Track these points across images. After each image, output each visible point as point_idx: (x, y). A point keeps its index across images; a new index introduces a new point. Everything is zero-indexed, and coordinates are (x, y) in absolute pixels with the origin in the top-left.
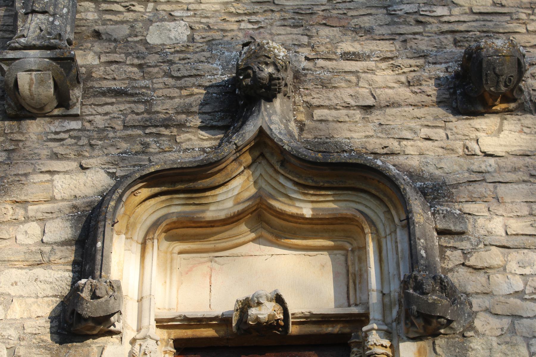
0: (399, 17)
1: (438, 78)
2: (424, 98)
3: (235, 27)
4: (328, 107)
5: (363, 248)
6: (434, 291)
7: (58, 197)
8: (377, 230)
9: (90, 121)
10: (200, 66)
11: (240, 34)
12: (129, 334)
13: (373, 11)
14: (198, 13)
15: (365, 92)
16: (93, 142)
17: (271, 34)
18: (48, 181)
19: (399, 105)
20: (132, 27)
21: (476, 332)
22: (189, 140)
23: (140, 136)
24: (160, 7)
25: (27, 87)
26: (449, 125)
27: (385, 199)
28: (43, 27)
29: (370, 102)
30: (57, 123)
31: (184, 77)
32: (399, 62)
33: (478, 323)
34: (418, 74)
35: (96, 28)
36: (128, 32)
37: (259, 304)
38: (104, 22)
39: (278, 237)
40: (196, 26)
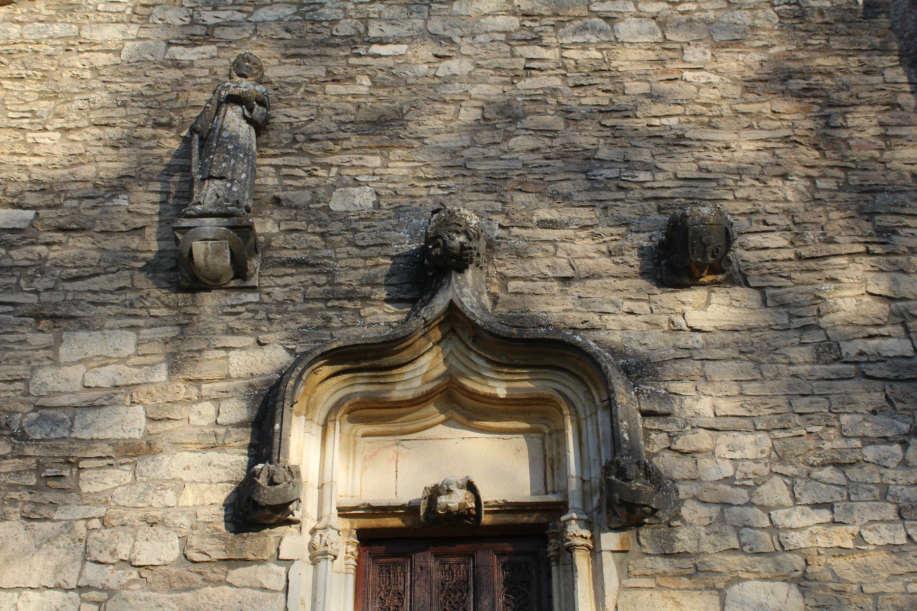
0: (599, 182)
1: (641, 248)
2: (627, 269)
4: (524, 279)
5: (562, 431)
6: (638, 477)
7: (234, 375)
8: (577, 412)
9: (268, 294)
10: (387, 234)
11: (430, 201)
12: (309, 524)
13: (572, 176)
14: (385, 178)
15: (563, 262)
16: (271, 316)
18: (223, 358)
19: (600, 277)
20: (314, 192)
21: (683, 521)
22: (375, 313)
23: (321, 309)
24: (344, 172)
25: (202, 257)
26: (653, 298)
27: (585, 378)
28: (221, 193)
29: (569, 273)
30: (233, 295)
31: (369, 246)
32: (600, 230)
33: (685, 512)
34: (620, 243)
35: (276, 194)
36: (309, 198)
37: (449, 491)
39: (470, 419)
40: (383, 192)
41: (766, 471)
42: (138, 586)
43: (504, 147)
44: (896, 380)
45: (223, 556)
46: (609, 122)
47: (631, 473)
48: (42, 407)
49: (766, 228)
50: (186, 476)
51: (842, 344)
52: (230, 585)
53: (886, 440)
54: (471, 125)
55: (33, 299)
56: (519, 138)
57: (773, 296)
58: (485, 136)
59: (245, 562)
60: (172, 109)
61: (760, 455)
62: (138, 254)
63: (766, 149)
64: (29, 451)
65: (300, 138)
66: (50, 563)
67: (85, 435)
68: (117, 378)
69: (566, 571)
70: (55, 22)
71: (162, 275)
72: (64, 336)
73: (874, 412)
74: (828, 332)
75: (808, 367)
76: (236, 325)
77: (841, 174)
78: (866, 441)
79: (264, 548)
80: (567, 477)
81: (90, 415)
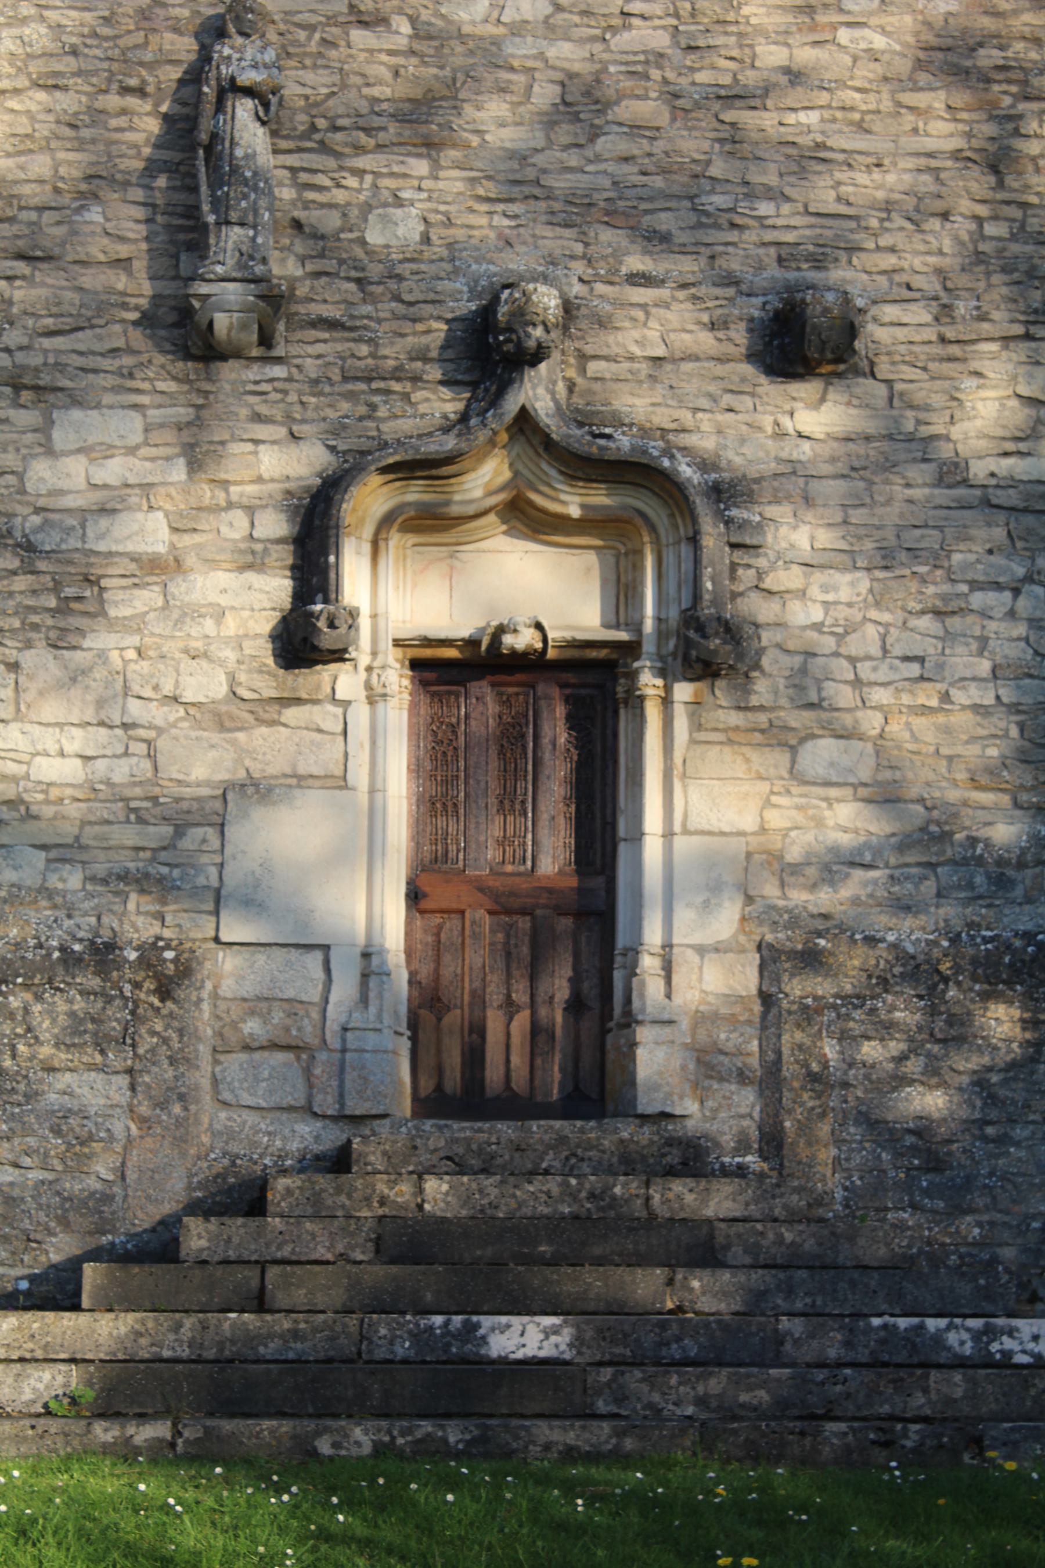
0: (707, 214)
1: (751, 320)
2: (731, 349)
3: (484, 221)
4: (606, 358)
5: (639, 553)
6: (716, 634)
8: (658, 538)
9: (298, 366)
10: (441, 285)
11: (492, 235)
12: (364, 660)
13: (672, 204)
14: (435, 195)
15: (653, 335)
16: (304, 399)
17: (534, 236)
19: (697, 359)
20: (345, 215)
21: (763, 672)
22: (427, 400)
23: (363, 392)
25: (225, 332)
26: (759, 390)
28: (244, 249)
29: (660, 351)
30: (256, 367)
33: (765, 662)
34: (726, 311)
35: (296, 214)
36: (338, 223)
37: (515, 631)
38: (307, 205)
40: (433, 218)
41: (859, 617)
42: (186, 724)
43: (589, 153)
44: (1025, 510)
45: (274, 694)
46: (728, 116)
47: (709, 631)
48: (44, 510)
49: (906, 294)
50: (224, 601)
51: (971, 462)
52: (285, 725)
53: (998, 586)
54: (546, 114)
56: (610, 137)
57: (902, 394)
58: (564, 134)
59: (298, 701)
60: (141, 64)
61: (855, 599)
62: (128, 299)
63: (929, 170)
64: (42, 565)
65: (321, 123)
66: (89, 698)
67: (102, 547)
68: (128, 474)
69: (634, 715)
71: (163, 333)
72: (55, 415)
73: (990, 552)
74: (960, 447)
75: (927, 491)
76: (264, 410)
77: (1016, 213)
78: (975, 586)
79: (318, 687)
80: (642, 617)
81: (104, 522)
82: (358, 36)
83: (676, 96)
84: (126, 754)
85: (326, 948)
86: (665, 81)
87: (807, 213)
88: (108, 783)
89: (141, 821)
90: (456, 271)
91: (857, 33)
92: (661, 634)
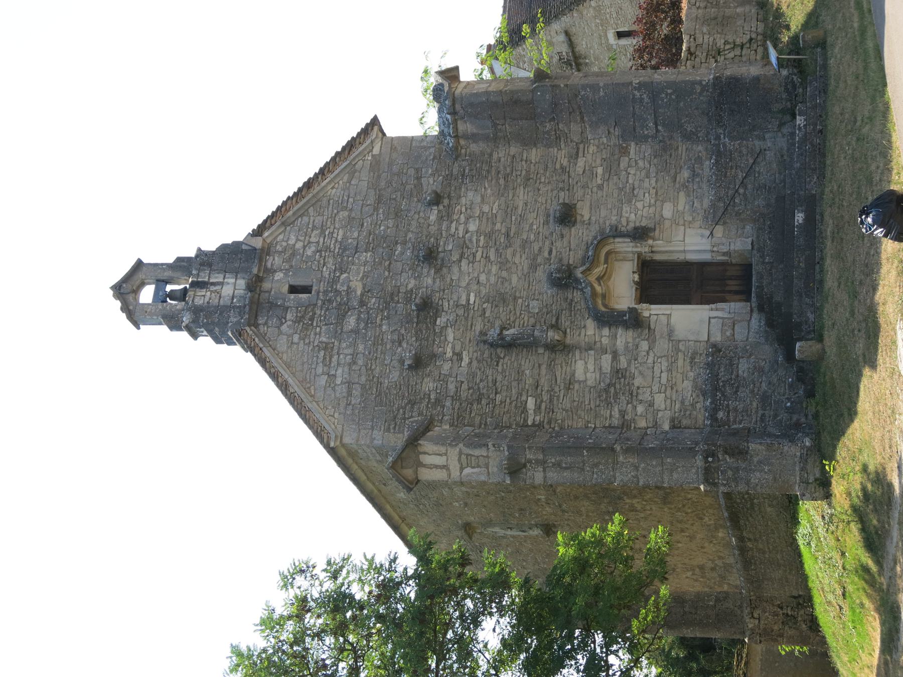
3: (534, 288)
29: (568, 249)
32: (554, 240)
50: (624, 341)
55: (562, 391)
59: (649, 325)
70: (444, 405)
76: (578, 333)
81: (603, 369)
82: (487, 315)
83: (506, 246)
84: (661, 363)
85: (710, 318)
86: (503, 249)
87: (536, 219)
88: (667, 367)
89: (677, 360)
90: (546, 292)
91: (494, 209)
92: (636, 247)
